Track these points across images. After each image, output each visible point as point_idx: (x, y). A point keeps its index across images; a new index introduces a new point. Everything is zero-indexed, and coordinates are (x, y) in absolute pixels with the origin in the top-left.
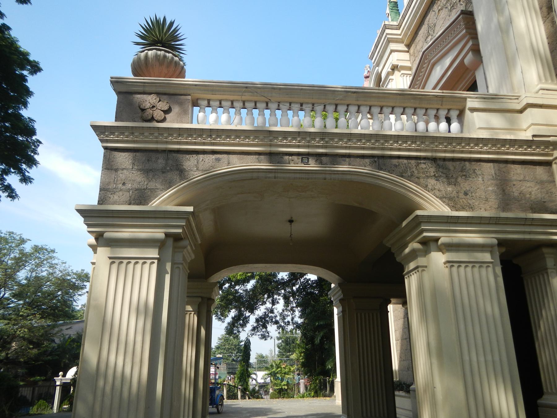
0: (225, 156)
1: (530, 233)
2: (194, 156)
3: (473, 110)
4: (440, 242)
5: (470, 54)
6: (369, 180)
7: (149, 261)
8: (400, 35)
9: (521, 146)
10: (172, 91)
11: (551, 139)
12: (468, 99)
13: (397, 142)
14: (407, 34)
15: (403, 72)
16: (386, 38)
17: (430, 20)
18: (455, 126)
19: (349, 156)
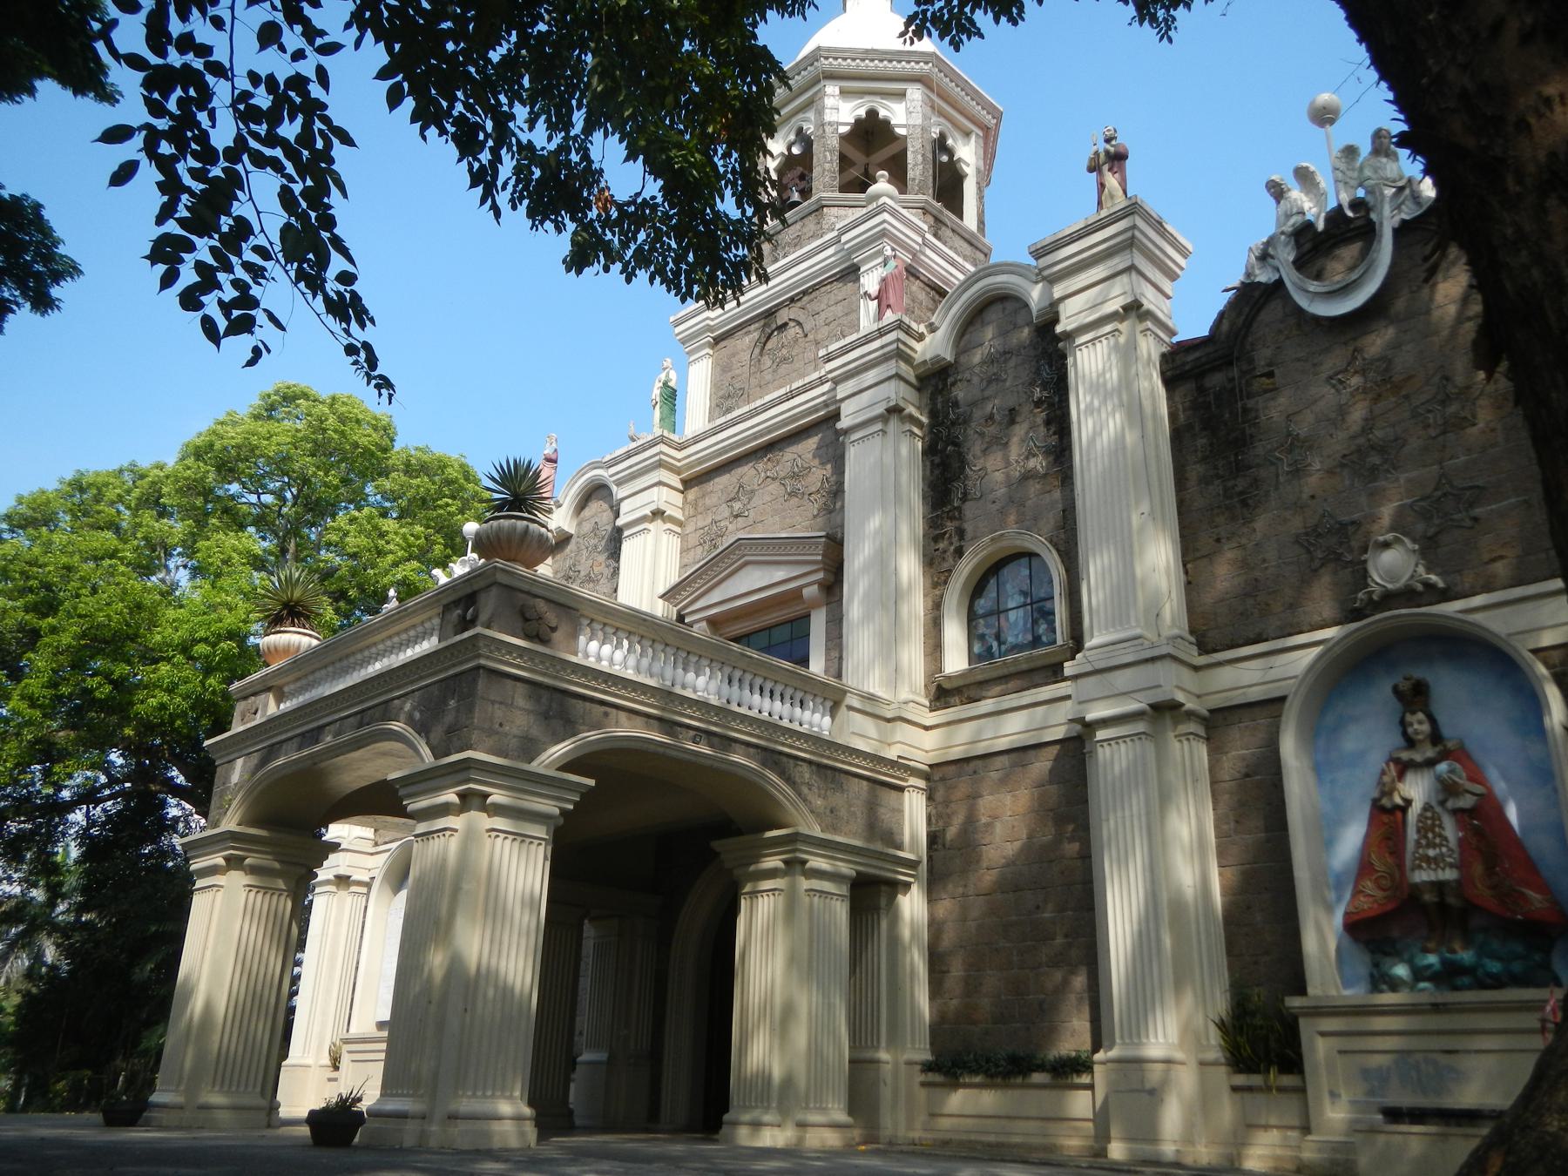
0: (614, 711)
3: (850, 708)
5: (816, 587)
6: (757, 779)
7: (536, 842)
9: (886, 766)
10: (562, 600)
11: (912, 763)
14: (692, 467)
15: (669, 526)
16: (657, 458)
17: (745, 479)
18: (827, 719)
19: (736, 741)
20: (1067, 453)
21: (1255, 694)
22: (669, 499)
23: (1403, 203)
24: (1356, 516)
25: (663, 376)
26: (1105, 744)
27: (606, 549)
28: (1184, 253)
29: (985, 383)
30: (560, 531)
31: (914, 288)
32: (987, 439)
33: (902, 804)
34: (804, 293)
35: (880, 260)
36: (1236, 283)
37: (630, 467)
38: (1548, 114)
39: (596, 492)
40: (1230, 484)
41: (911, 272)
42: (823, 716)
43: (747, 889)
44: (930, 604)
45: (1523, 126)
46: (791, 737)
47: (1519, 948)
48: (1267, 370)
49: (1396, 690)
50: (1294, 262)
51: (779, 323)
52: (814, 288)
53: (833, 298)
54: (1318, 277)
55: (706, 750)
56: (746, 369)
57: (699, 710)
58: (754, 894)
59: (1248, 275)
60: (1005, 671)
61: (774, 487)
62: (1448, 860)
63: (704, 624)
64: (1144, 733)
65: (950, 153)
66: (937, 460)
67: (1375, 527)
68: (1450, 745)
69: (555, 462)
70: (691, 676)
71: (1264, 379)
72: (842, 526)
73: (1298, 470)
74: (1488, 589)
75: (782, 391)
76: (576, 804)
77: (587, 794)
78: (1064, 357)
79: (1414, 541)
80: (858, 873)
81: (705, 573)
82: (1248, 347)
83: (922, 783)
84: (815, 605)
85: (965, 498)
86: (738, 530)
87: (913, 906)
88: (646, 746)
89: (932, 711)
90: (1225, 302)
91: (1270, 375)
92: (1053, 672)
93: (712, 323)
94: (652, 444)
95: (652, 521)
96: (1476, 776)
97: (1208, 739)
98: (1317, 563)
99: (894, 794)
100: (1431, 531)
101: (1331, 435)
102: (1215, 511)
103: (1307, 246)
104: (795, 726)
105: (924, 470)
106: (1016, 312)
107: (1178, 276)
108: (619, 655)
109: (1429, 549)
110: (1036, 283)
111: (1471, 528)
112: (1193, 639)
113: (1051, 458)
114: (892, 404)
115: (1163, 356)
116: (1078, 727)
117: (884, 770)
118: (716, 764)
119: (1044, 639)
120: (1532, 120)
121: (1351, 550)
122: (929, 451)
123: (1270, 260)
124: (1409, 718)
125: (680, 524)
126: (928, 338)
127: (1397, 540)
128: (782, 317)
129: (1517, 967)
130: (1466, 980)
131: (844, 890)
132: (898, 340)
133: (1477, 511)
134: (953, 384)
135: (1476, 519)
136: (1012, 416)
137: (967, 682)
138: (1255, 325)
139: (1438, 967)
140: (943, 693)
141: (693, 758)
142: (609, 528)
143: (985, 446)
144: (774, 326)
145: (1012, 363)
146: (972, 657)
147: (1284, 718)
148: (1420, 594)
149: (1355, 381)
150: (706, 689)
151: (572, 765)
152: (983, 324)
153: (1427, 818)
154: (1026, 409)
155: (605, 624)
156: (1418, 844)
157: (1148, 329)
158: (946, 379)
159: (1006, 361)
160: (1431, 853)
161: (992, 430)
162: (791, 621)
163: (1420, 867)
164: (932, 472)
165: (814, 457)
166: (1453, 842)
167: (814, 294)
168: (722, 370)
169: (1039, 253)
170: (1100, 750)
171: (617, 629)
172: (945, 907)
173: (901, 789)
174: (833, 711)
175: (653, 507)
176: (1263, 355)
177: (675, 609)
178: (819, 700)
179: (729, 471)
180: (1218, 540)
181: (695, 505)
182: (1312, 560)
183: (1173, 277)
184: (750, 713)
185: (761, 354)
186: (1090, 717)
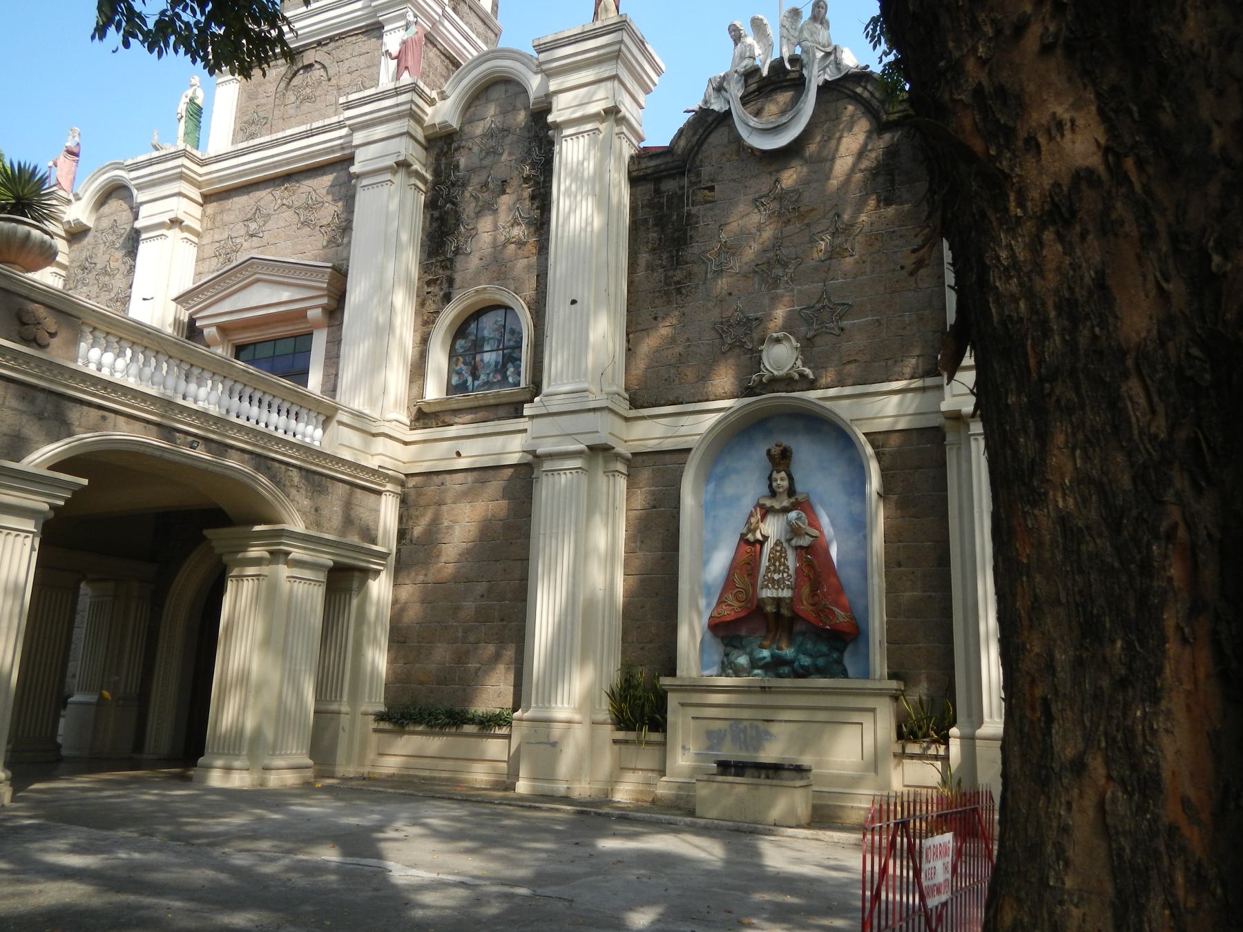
0: (113, 415)
2: (78, 405)
3: (340, 423)
4: (290, 556)
5: (319, 310)
6: (249, 481)
7: (23, 534)
9: (367, 473)
11: (390, 472)
12: (340, 411)
13: (277, 444)
15: (187, 235)
16: (178, 170)
17: (262, 203)
18: (319, 432)
19: (232, 447)
20: (545, 226)
21: (668, 445)
22: (190, 212)
23: (827, 66)
24: (759, 314)
25: (190, 93)
26: (549, 474)
27: (123, 246)
28: (659, 72)
29: (484, 154)
30: (78, 222)
31: (431, 55)
32: (480, 203)
33: (379, 505)
34: (331, 39)
35: (403, 23)
36: (696, 107)
37: (152, 174)
38: (1058, 138)
39: (115, 191)
40: (671, 273)
41: (430, 39)
42: (316, 428)
43: (235, 572)
44: (418, 339)
45: (1032, 144)
46: (284, 447)
47: (824, 648)
48: (709, 184)
49: (769, 452)
50: (741, 98)
51: (306, 63)
52: (341, 37)
53: (357, 50)
54: (757, 114)
55: (201, 453)
56: (271, 100)
57: (198, 418)
58: (240, 577)
59: (706, 102)
60: (476, 404)
61: (288, 214)
62: (787, 583)
63: (214, 329)
64: (580, 468)
66: (436, 214)
67: (771, 325)
68: (800, 498)
69: (77, 155)
70: (192, 387)
71: (706, 191)
72: (348, 259)
73: (722, 271)
74: (841, 383)
75: (303, 128)
76: (67, 501)
77: (79, 492)
78: (552, 143)
80: (335, 562)
81: (218, 283)
82: (698, 163)
83: (399, 489)
84: (318, 326)
85: (457, 252)
86: (252, 248)
87: (380, 588)
88: (142, 449)
89: (411, 429)
90: (685, 121)
91: (711, 189)
92: (516, 411)
94: (175, 156)
95: (170, 228)
96: (814, 523)
97: (628, 476)
98: (725, 348)
99: (373, 496)
100: (810, 335)
101: (750, 247)
102: (657, 294)
103: (754, 87)
104: (289, 438)
105: (424, 222)
106: (516, 95)
107: (651, 91)
108: (121, 363)
109: (807, 347)
110: (536, 73)
111: (839, 335)
112: (627, 396)
113: (532, 229)
114: (401, 158)
115: (632, 157)
116: (530, 457)
118: (211, 468)
119: (510, 380)
120: (1042, 140)
121: (752, 341)
122: (431, 205)
123: (723, 92)
124: (775, 475)
125: (198, 234)
126: (439, 104)
127: (786, 338)
128: (309, 57)
129: (821, 662)
130: (786, 669)
131: (322, 577)
132: (412, 101)
133: (844, 323)
134: (457, 149)
135: (842, 329)
136: (503, 186)
137: (443, 408)
138: (705, 146)
139: (769, 659)
140: (424, 417)
141: (189, 461)
142: (128, 228)
143: (477, 210)
144: (300, 65)
145: (508, 140)
146: (451, 389)
147: (687, 466)
148: (796, 381)
149: (774, 206)
150: (207, 399)
151: (63, 465)
152: (488, 101)
153: (777, 551)
154: (515, 182)
155: (108, 333)
156: (768, 568)
157: (623, 133)
158: (450, 144)
159: (504, 137)
160: (776, 577)
161: (486, 196)
162: (296, 337)
163: (767, 586)
164: (431, 224)
165: (328, 193)
166: (792, 572)
167: (340, 43)
168: (248, 97)
169: (541, 48)
170: (544, 478)
171: (121, 338)
172: (406, 592)
173: (379, 493)
174: (325, 424)
175: (172, 215)
176: (706, 171)
177: (187, 313)
178: (313, 414)
179: (248, 193)
180: (655, 318)
181: (213, 218)
182: (723, 344)
183: (647, 91)
184: (247, 424)
185: (286, 88)
186: (540, 451)
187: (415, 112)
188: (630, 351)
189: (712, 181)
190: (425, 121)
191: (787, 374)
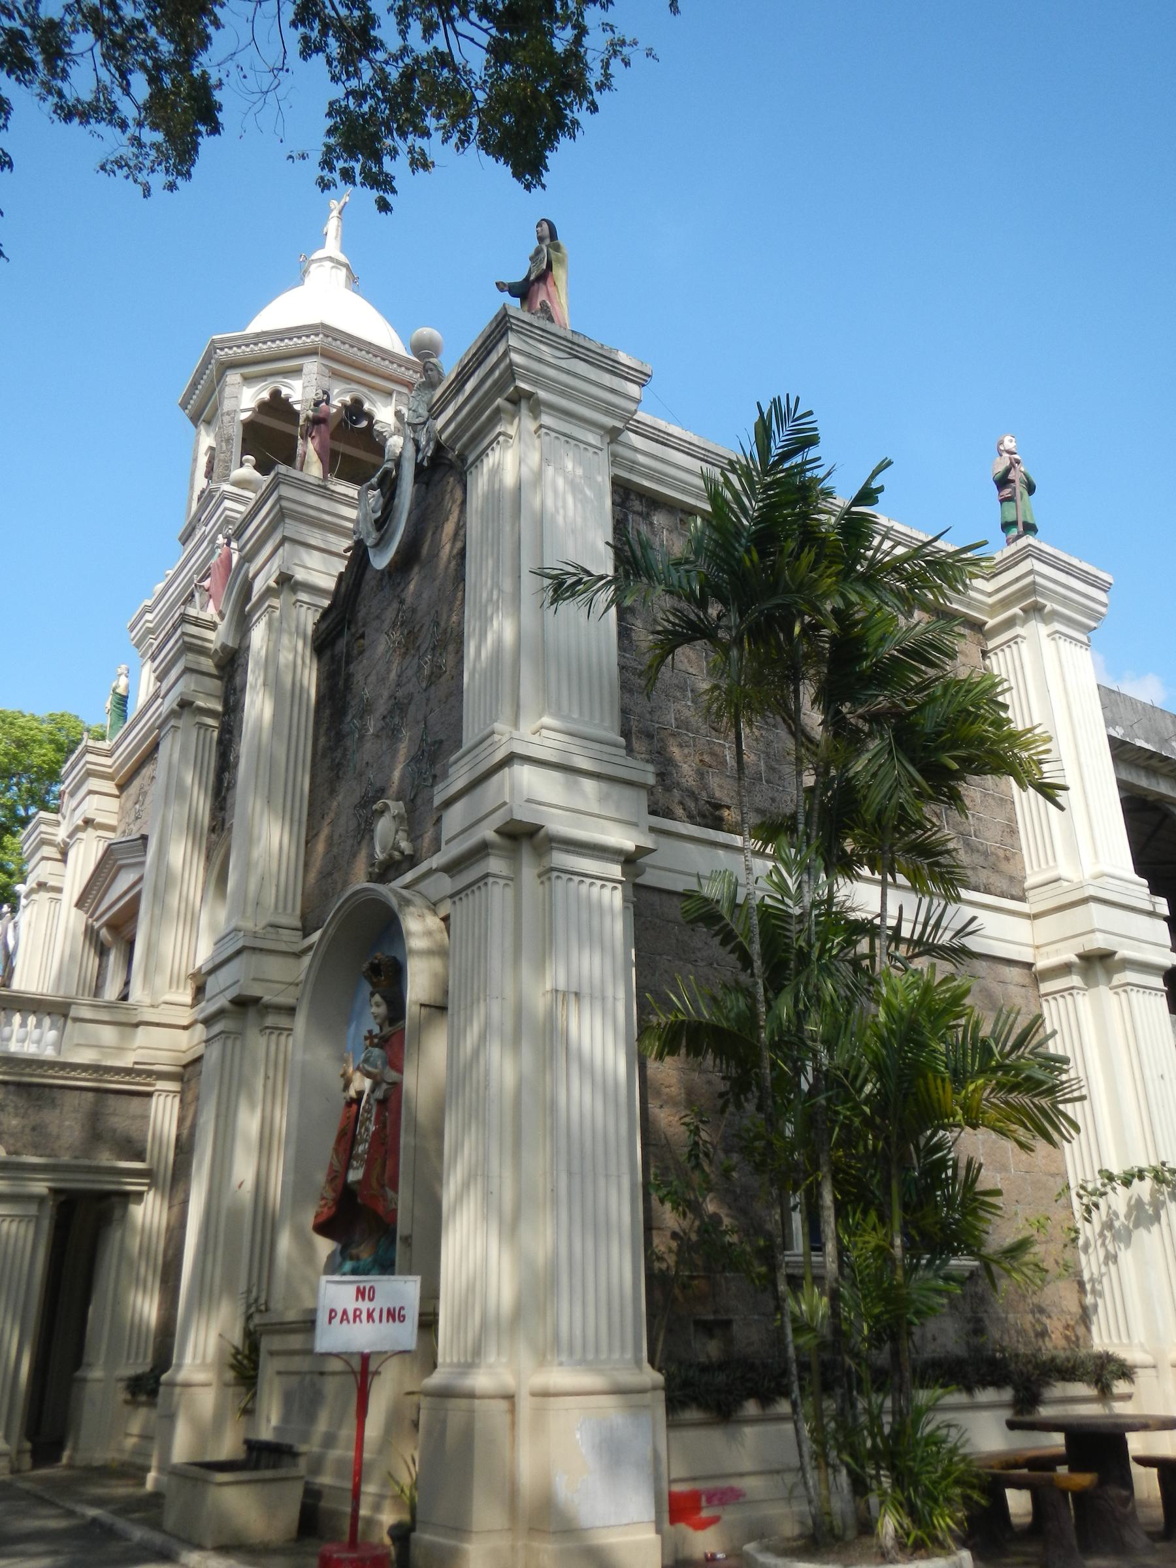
1: (93, 1181)
8: (110, 767)
11: (155, 1068)
18: (52, 1035)
25: (114, 685)
33: (148, 1109)
48: (360, 632)
65: (369, 416)
79: (405, 804)
85: (228, 789)
91: (362, 636)
93: (151, 625)
99: (136, 1101)
117: (116, 1078)
122: (220, 741)
125: (112, 829)
132: (183, 634)
173: (149, 1095)
187: (191, 644)
188: (306, 865)
189: (364, 626)
190: (210, 649)
191: (391, 856)
